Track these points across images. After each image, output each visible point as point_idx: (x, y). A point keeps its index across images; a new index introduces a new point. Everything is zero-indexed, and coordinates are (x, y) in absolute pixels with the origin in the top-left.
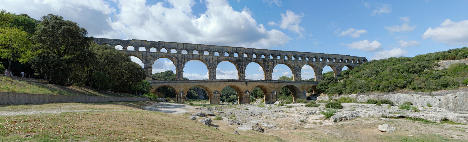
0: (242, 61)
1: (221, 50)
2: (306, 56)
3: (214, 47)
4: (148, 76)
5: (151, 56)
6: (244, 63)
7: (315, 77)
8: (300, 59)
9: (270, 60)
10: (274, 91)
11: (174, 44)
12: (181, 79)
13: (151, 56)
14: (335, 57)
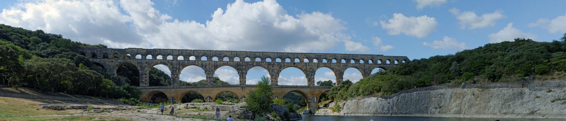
0: (242, 65)
2: (322, 57)
4: (143, 82)
5: (146, 63)
6: (244, 67)
8: (315, 61)
9: (276, 64)
12: (176, 84)
13: (146, 63)
14: (362, 57)
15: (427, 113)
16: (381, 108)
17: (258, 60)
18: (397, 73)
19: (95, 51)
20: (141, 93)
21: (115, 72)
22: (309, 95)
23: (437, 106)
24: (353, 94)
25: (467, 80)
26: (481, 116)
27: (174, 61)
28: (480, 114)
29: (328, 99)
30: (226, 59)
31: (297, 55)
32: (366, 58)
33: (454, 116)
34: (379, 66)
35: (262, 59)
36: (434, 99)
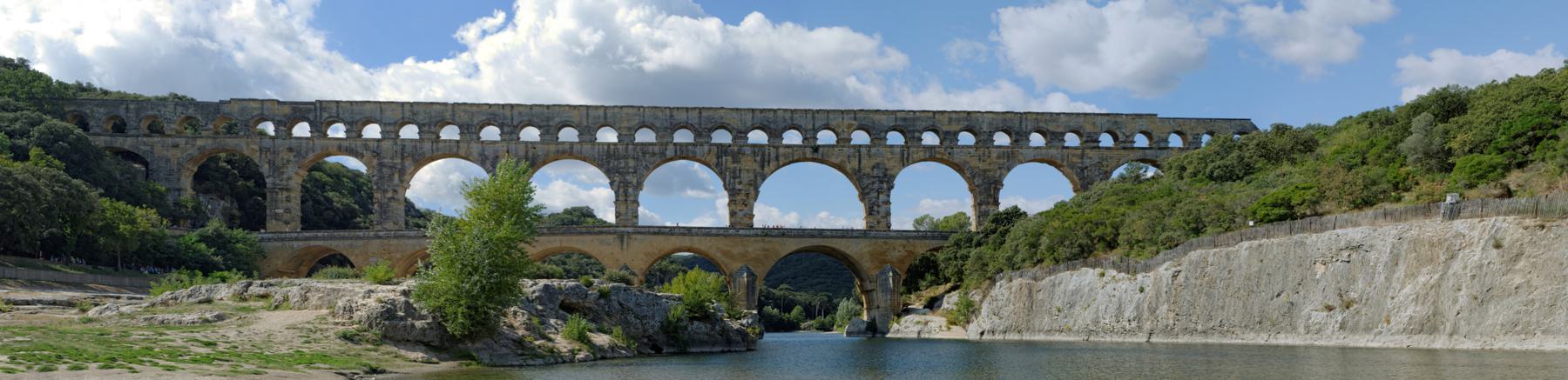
0: (626, 157)
1: (549, 117)
2: (920, 125)
3: (515, 111)
4: (276, 217)
5: (290, 150)
6: (632, 163)
7: (970, 212)
8: (895, 138)
9: (748, 151)
10: (740, 272)
11: (368, 107)
13: (290, 150)
14: (1073, 124)
15: (1294, 329)
16: (1112, 309)
17: (683, 137)
18: (1195, 174)
19: (122, 112)
20: (262, 254)
21: (187, 182)
22: (867, 265)
23: (1334, 300)
24: (1019, 257)
25: (1471, 186)
26: (1532, 344)
27: (387, 145)
28: (1528, 332)
29: (947, 280)
30: (568, 135)
31: (825, 119)
32: (1088, 128)
33: (1404, 341)
34: (1139, 154)
35: (698, 134)
36: (1320, 269)
